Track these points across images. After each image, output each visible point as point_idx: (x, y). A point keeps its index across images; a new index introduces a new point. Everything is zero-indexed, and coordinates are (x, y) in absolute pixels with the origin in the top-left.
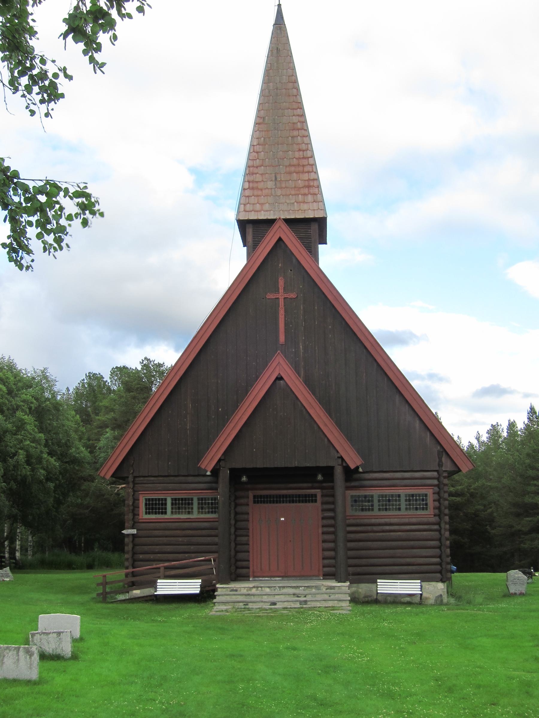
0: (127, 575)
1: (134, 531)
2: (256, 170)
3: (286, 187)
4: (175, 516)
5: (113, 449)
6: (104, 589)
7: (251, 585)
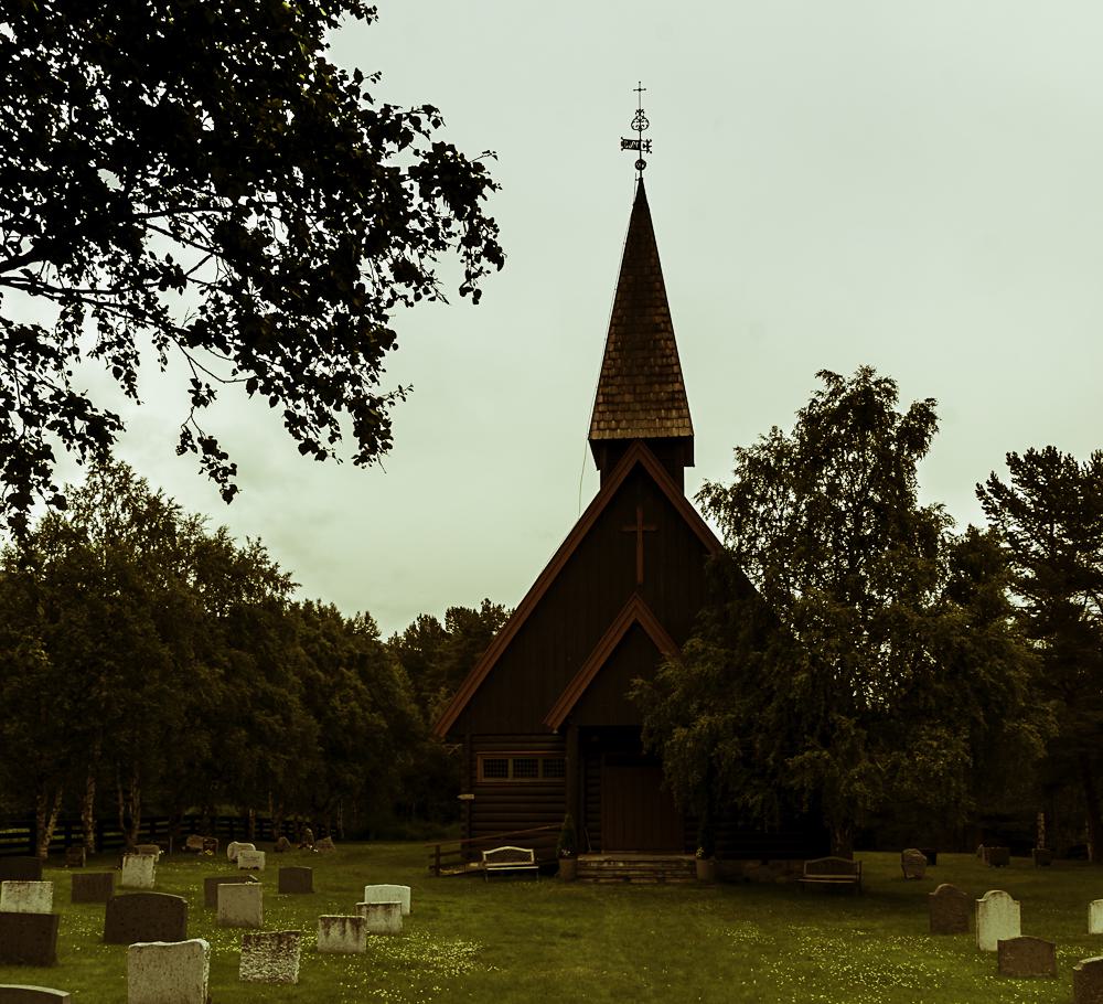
0: (463, 846)
1: (472, 797)
2: (611, 381)
3: (646, 401)
4: (517, 780)
5: (445, 708)
6: (438, 860)
7: (602, 859)
